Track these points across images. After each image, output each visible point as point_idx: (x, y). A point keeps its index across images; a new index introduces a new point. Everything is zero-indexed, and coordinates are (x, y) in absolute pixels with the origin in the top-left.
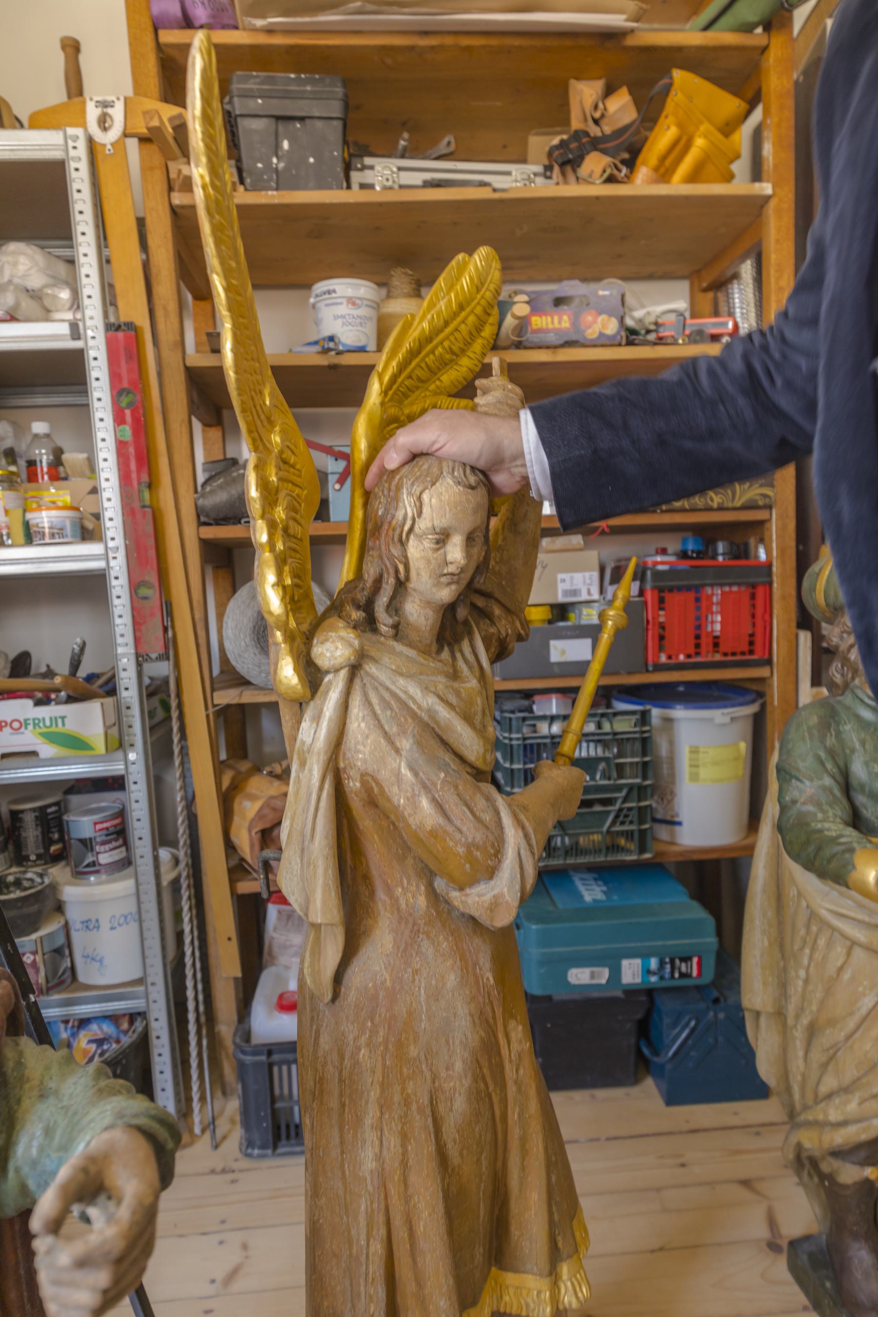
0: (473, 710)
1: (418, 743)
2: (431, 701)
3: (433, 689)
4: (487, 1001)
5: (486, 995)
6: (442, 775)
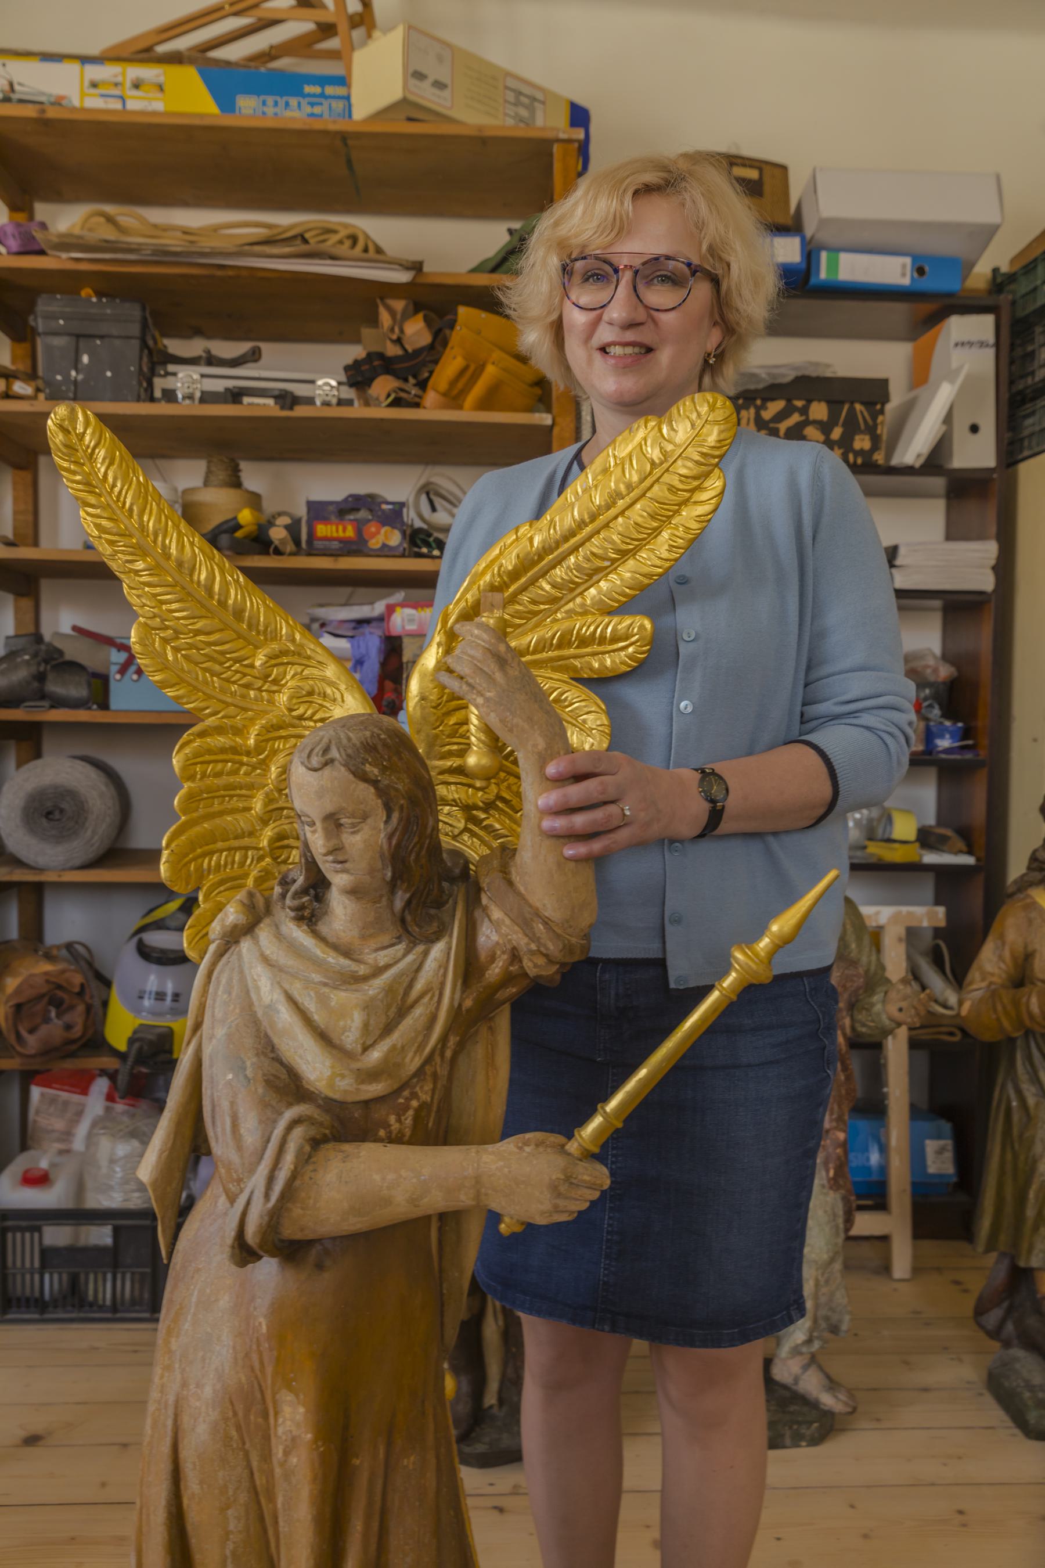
0: (342, 1023)
1: (229, 1036)
2: (278, 996)
3: (287, 986)
4: (254, 1347)
5: (255, 1340)
6: (230, 1076)
